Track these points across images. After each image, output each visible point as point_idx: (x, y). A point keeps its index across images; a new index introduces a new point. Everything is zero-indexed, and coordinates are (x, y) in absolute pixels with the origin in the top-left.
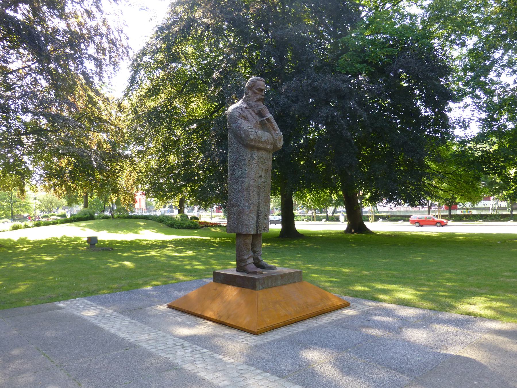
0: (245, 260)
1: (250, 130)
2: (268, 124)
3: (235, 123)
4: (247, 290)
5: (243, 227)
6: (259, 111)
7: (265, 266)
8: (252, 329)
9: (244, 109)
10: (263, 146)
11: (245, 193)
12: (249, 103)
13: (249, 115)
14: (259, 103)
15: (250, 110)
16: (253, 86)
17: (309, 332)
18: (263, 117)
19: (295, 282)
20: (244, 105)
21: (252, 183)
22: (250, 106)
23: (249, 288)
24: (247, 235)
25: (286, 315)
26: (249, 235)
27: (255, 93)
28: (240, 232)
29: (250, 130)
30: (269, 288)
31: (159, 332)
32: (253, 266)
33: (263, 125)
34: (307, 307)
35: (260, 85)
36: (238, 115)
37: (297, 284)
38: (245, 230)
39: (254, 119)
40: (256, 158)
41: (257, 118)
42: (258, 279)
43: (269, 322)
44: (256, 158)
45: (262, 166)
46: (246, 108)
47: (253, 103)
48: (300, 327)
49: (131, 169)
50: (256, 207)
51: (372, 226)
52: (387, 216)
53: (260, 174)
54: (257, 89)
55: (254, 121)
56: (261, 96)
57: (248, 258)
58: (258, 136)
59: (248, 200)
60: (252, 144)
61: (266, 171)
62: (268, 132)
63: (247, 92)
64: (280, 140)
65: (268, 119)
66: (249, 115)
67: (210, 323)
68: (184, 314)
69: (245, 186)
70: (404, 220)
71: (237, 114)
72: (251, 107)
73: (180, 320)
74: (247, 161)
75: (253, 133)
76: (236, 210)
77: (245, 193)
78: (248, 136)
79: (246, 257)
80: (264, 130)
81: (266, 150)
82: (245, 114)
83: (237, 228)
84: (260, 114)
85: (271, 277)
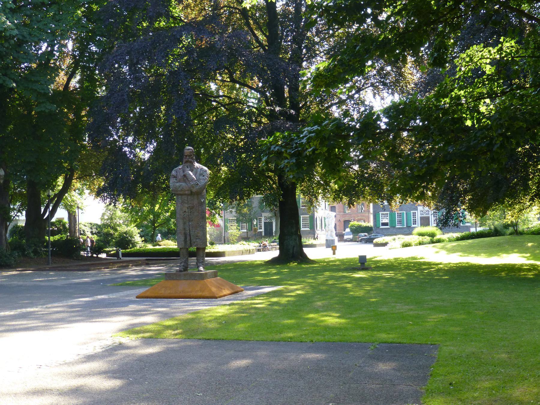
10: (181, 193)
81: (186, 194)
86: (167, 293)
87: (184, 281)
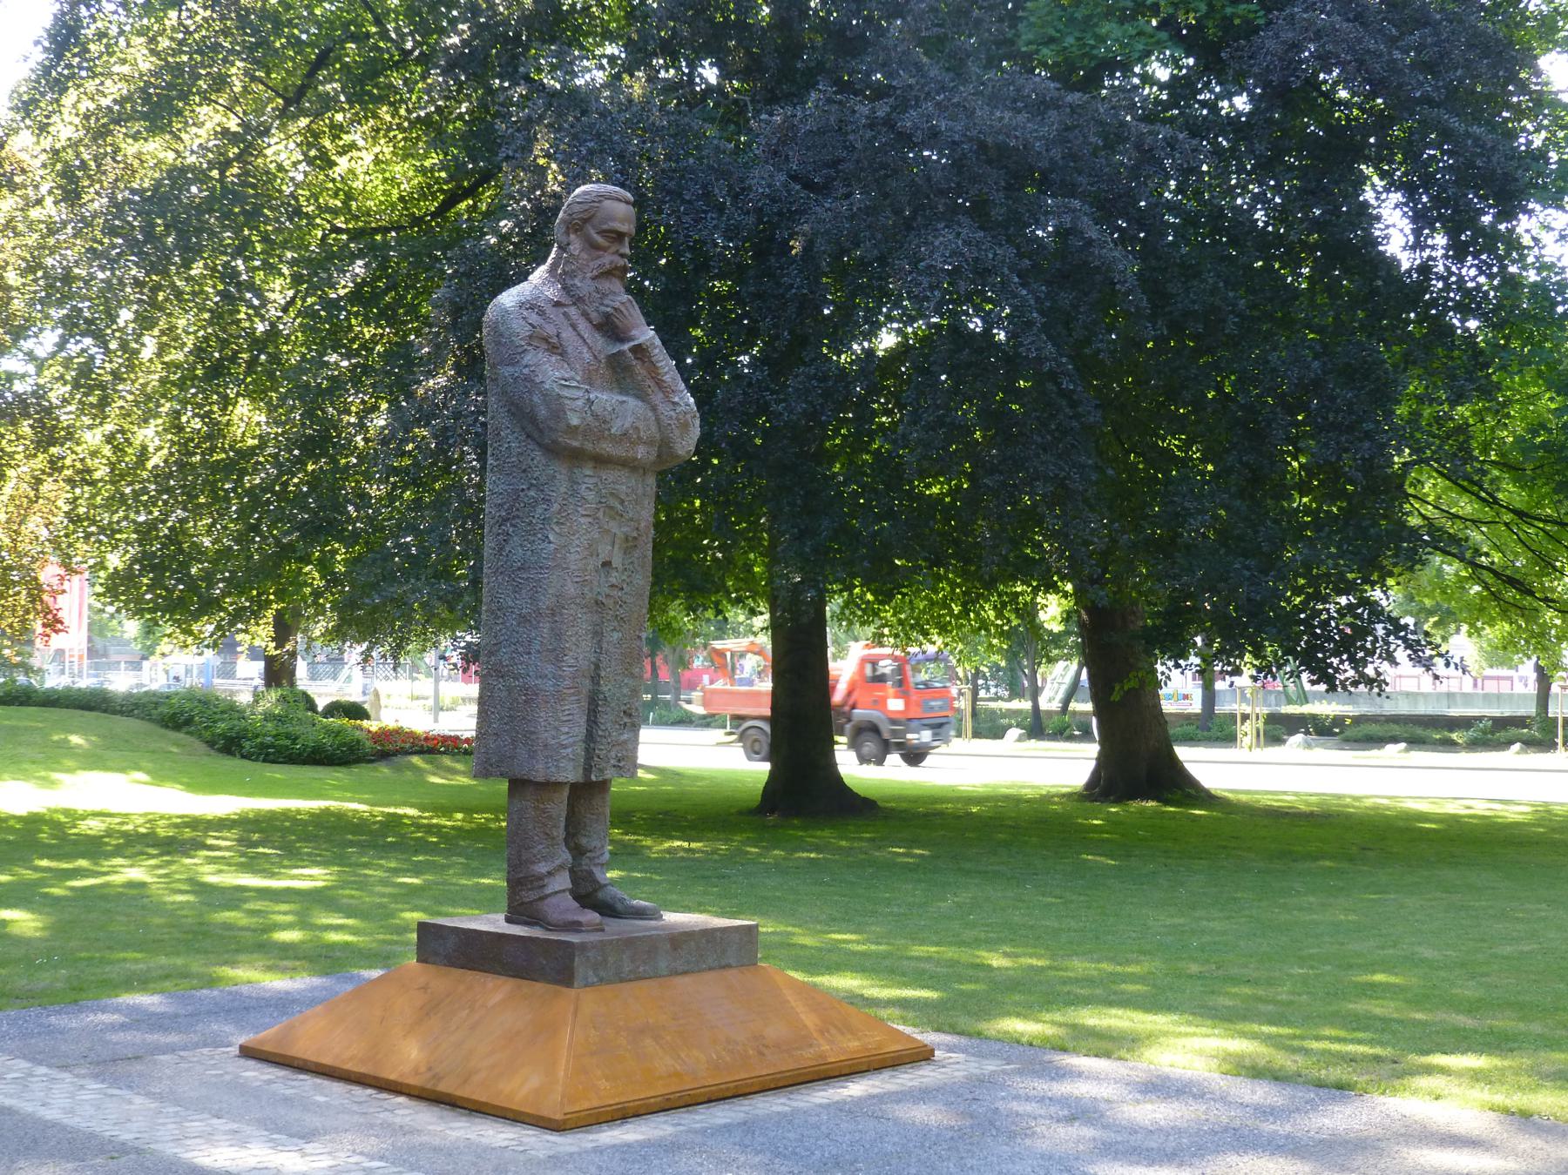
0: (540, 878)
1: (566, 393)
2: (639, 368)
3: (512, 362)
4: (540, 987)
5: (532, 755)
6: (607, 316)
7: (619, 906)
8: (546, 1113)
9: (549, 310)
11: (545, 628)
12: (569, 282)
13: (567, 334)
14: (605, 285)
15: (573, 311)
16: (585, 221)
17: (748, 1127)
18: (622, 340)
19: (729, 966)
20: (552, 292)
21: (571, 590)
22: (572, 296)
23: (549, 982)
24: (549, 786)
25: (677, 1074)
26: (558, 785)
27: (595, 246)
28: (522, 772)
29: (566, 393)
30: (622, 980)
31: (215, 1121)
32: (569, 901)
33: (622, 371)
34: (761, 1054)
35: (613, 219)
36: (525, 331)
37: (732, 975)
38: (540, 766)
39: (587, 345)
40: (591, 496)
41: (599, 341)
42: (583, 947)
43: (607, 1093)
44: (591, 496)
45: (613, 526)
46: (557, 304)
47: (584, 285)
48: (722, 1115)
49: (40, 461)
50: (587, 682)
51: (1206, 765)
52: (1338, 721)
53: (603, 557)
54: (602, 233)
55: (587, 356)
56: (616, 258)
57: (550, 874)
58: (595, 416)
59: (557, 656)
60: (575, 444)
61: (630, 544)
62: (637, 397)
63: (564, 239)
64: (685, 426)
65: (640, 351)
66: (567, 334)
67: (401, 1099)
68: (302, 1077)
69: (546, 602)
70: (1415, 742)
71: (520, 328)
72: (578, 301)
73: (289, 1092)
74: (556, 507)
75: (580, 403)
76: (510, 690)
77: (545, 628)
78: (558, 413)
79: (542, 868)
80: (623, 391)
82: (550, 330)
83: (512, 758)
84: (610, 328)
85: (630, 942)
86: (698, 1064)
87: (687, 979)
